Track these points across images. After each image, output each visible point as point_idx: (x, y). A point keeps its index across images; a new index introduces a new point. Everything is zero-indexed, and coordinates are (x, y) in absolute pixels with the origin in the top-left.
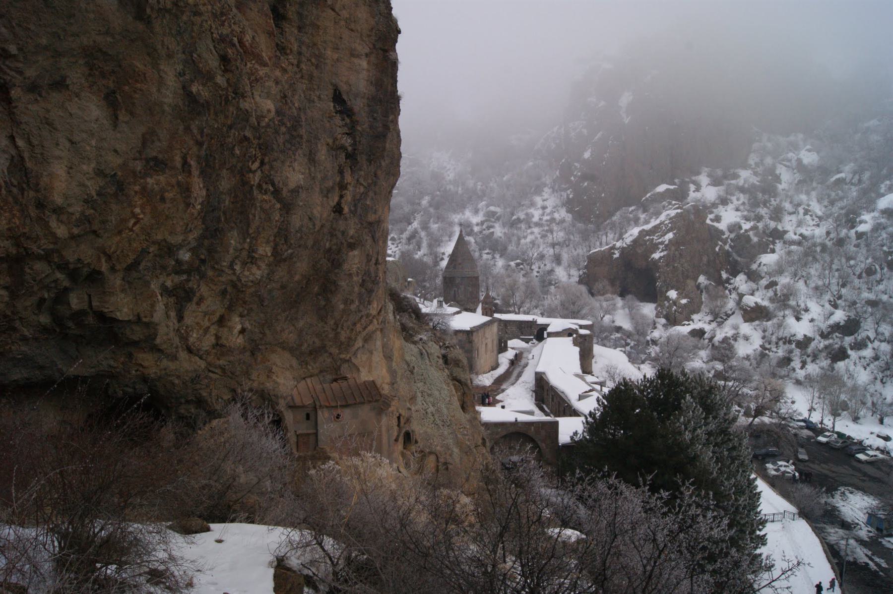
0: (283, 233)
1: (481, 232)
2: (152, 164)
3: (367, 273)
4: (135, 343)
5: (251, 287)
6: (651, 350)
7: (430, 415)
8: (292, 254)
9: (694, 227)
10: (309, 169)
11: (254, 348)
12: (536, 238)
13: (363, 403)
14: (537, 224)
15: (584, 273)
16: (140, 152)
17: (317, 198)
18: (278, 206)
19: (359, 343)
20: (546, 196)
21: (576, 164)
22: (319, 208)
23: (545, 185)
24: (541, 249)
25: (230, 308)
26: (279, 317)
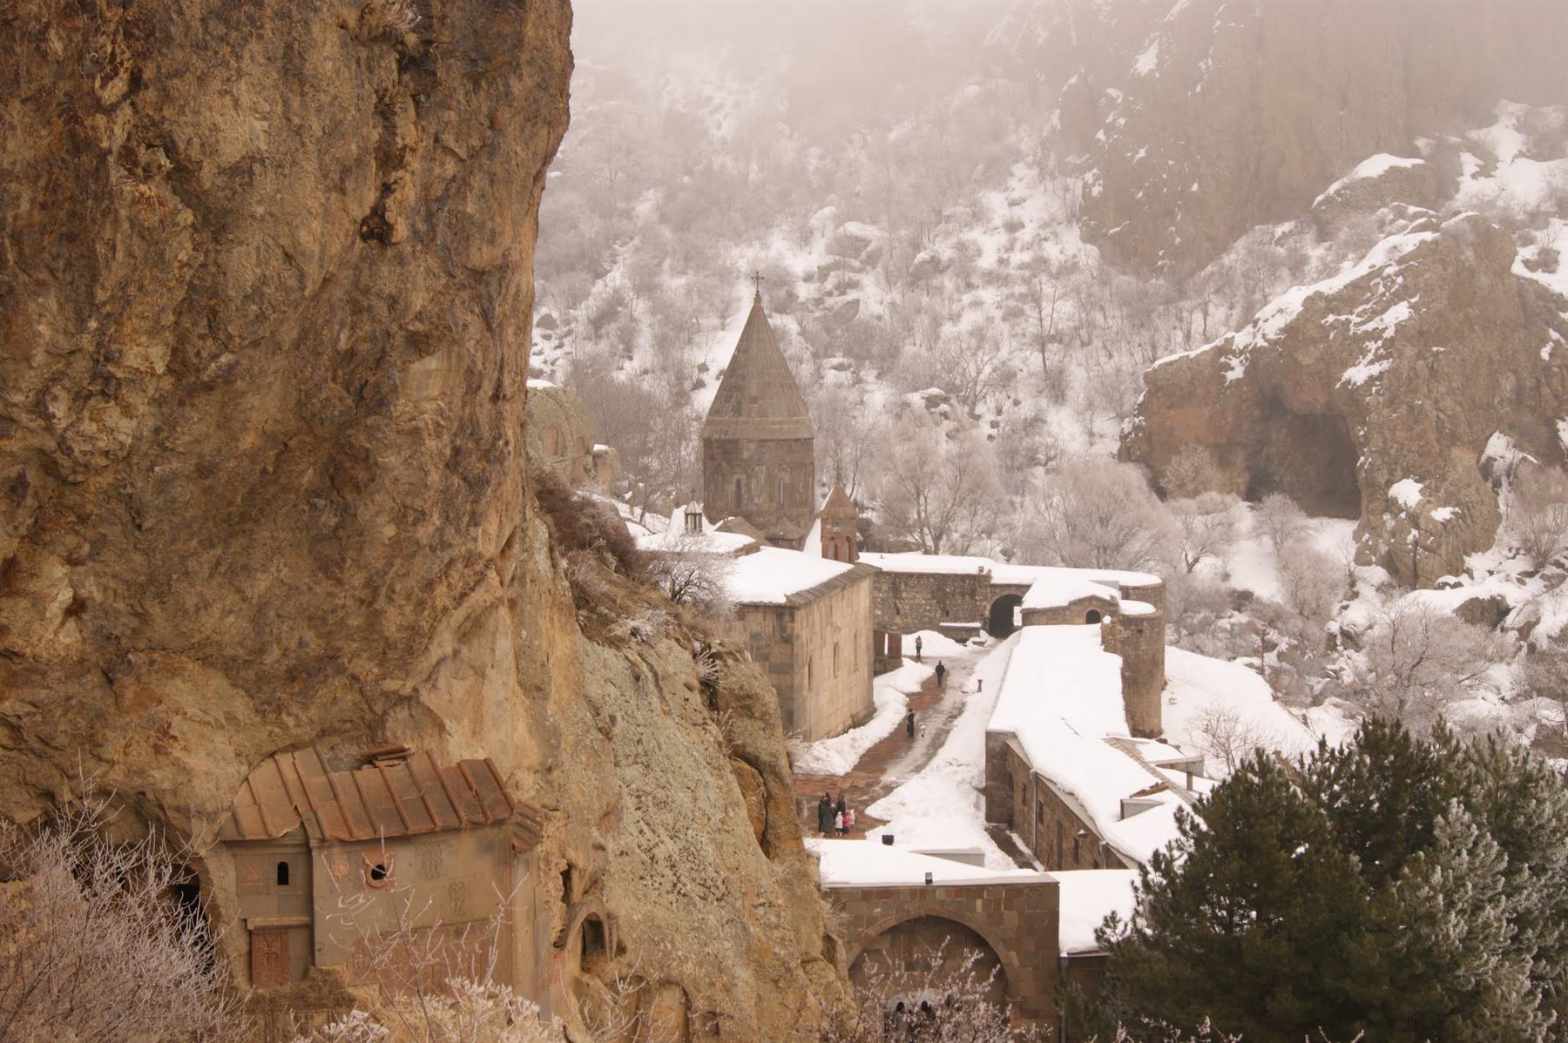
0: (203, 303)
1: (819, 302)
3: (469, 427)
5: (98, 472)
6: (1341, 663)
7: (662, 867)
8: (231, 367)
10: (286, 103)
11: (112, 663)
12: (990, 319)
14: (991, 278)
15: (1137, 428)
17: (309, 191)
18: (187, 217)
19: (445, 642)
20: (1018, 189)
21: (1111, 91)
22: (316, 225)
23: (1017, 156)
24: (1003, 353)
25: (35, 538)
26: (192, 564)
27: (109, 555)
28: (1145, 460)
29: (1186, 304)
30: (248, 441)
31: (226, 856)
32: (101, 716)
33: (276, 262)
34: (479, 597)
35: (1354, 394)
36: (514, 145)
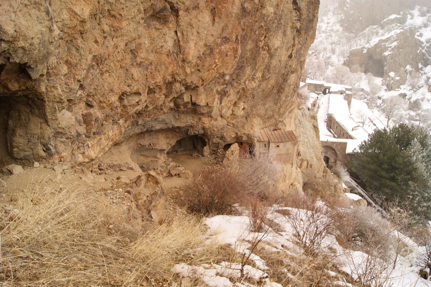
0: (268, 68)
2: (224, 40)
4: (203, 114)
5: (250, 90)
7: (305, 143)
9: (409, 39)
12: (323, 39)
13: (288, 141)
14: (324, 32)
15: (347, 60)
16: (220, 35)
19: (287, 113)
25: (239, 99)
26: (259, 103)
27: (249, 102)
28: (348, 65)
29: (357, 39)
30: (269, 86)
31: (258, 143)
32: (245, 123)
33: (278, 62)
34: (292, 107)
35: (385, 57)
36: (308, 42)
